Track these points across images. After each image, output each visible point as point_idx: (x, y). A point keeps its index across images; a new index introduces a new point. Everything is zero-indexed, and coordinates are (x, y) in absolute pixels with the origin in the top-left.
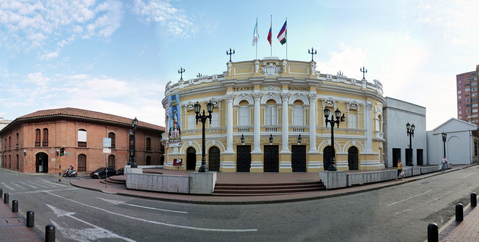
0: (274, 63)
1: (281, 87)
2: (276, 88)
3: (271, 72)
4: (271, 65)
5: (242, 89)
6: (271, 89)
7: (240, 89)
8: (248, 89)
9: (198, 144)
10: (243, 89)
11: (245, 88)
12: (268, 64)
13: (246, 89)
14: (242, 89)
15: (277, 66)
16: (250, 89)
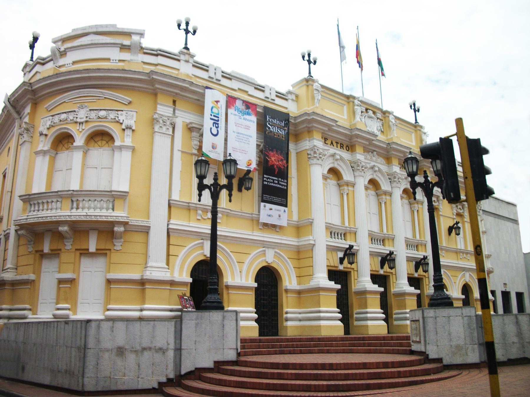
0: (374, 113)
1: (388, 160)
2: (381, 160)
3: (373, 126)
4: (370, 113)
5: (332, 143)
6: (374, 158)
7: (329, 142)
8: (342, 146)
9: (236, 263)
10: (335, 144)
11: (337, 143)
12: (367, 110)
13: (339, 145)
14: (332, 143)
15: (378, 118)
16: (344, 147)
